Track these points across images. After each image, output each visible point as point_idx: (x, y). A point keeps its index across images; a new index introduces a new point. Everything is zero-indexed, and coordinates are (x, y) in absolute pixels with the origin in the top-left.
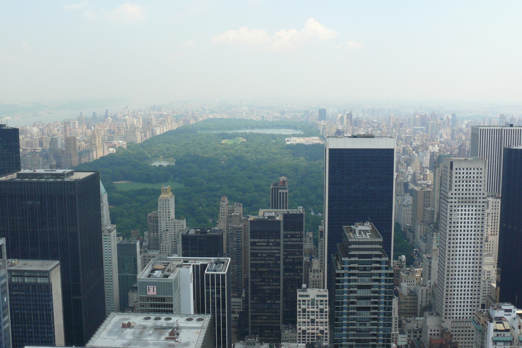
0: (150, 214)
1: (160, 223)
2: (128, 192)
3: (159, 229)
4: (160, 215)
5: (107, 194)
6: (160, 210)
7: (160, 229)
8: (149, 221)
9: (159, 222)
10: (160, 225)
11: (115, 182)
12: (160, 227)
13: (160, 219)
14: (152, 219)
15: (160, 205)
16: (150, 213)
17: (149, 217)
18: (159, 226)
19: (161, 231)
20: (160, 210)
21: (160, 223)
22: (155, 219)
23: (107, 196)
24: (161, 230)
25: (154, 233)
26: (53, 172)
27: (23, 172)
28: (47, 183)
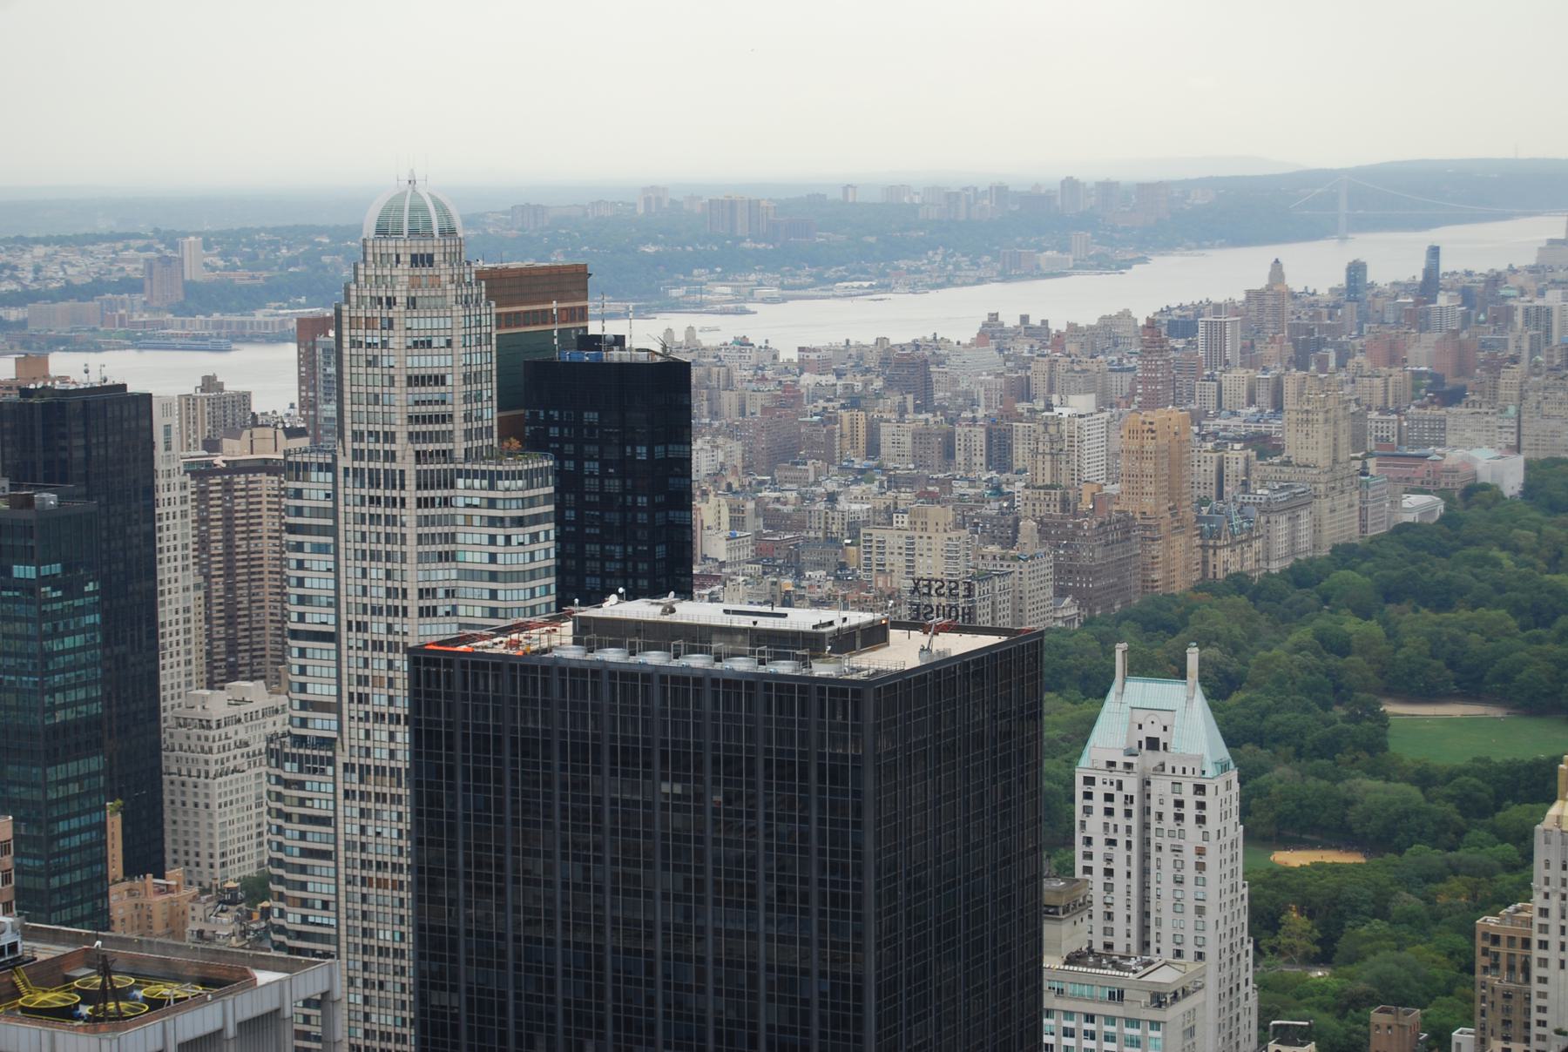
0: (1492, 920)
1: (1543, 980)
2: (1451, 776)
3: (1535, 1016)
4: (1544, 928)
5: (1233, 775)
6: (1547, 896)
7: (1542, 1016)
8: (1481, 961)
9: (1536, 971)
10: (1543, 995)
11: (1391, 708)
12: (1542, 1009)
13: (1543, 954)
14: (1503, 949)
15: (1547, 865)
16: (1496, 915)
17: (1485, 936)
18: (1536, 1002)
19: (1541, 1030)
20: (1547, 896)
21: (1543, 980)
22: (1518, 951)
23: (1236, 787)
24: (1542, 1023)
25: (1506, 1039)
26: (765, 623)
27: (617, 615)
28: (715, 682)
